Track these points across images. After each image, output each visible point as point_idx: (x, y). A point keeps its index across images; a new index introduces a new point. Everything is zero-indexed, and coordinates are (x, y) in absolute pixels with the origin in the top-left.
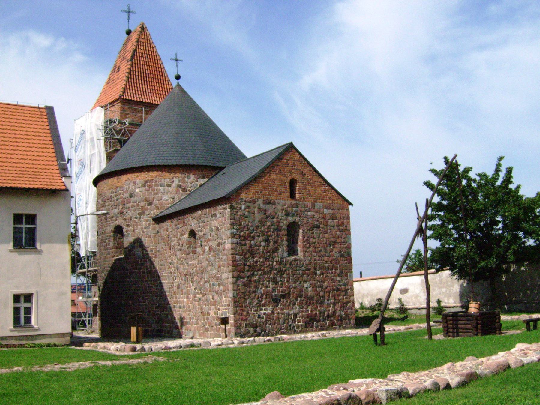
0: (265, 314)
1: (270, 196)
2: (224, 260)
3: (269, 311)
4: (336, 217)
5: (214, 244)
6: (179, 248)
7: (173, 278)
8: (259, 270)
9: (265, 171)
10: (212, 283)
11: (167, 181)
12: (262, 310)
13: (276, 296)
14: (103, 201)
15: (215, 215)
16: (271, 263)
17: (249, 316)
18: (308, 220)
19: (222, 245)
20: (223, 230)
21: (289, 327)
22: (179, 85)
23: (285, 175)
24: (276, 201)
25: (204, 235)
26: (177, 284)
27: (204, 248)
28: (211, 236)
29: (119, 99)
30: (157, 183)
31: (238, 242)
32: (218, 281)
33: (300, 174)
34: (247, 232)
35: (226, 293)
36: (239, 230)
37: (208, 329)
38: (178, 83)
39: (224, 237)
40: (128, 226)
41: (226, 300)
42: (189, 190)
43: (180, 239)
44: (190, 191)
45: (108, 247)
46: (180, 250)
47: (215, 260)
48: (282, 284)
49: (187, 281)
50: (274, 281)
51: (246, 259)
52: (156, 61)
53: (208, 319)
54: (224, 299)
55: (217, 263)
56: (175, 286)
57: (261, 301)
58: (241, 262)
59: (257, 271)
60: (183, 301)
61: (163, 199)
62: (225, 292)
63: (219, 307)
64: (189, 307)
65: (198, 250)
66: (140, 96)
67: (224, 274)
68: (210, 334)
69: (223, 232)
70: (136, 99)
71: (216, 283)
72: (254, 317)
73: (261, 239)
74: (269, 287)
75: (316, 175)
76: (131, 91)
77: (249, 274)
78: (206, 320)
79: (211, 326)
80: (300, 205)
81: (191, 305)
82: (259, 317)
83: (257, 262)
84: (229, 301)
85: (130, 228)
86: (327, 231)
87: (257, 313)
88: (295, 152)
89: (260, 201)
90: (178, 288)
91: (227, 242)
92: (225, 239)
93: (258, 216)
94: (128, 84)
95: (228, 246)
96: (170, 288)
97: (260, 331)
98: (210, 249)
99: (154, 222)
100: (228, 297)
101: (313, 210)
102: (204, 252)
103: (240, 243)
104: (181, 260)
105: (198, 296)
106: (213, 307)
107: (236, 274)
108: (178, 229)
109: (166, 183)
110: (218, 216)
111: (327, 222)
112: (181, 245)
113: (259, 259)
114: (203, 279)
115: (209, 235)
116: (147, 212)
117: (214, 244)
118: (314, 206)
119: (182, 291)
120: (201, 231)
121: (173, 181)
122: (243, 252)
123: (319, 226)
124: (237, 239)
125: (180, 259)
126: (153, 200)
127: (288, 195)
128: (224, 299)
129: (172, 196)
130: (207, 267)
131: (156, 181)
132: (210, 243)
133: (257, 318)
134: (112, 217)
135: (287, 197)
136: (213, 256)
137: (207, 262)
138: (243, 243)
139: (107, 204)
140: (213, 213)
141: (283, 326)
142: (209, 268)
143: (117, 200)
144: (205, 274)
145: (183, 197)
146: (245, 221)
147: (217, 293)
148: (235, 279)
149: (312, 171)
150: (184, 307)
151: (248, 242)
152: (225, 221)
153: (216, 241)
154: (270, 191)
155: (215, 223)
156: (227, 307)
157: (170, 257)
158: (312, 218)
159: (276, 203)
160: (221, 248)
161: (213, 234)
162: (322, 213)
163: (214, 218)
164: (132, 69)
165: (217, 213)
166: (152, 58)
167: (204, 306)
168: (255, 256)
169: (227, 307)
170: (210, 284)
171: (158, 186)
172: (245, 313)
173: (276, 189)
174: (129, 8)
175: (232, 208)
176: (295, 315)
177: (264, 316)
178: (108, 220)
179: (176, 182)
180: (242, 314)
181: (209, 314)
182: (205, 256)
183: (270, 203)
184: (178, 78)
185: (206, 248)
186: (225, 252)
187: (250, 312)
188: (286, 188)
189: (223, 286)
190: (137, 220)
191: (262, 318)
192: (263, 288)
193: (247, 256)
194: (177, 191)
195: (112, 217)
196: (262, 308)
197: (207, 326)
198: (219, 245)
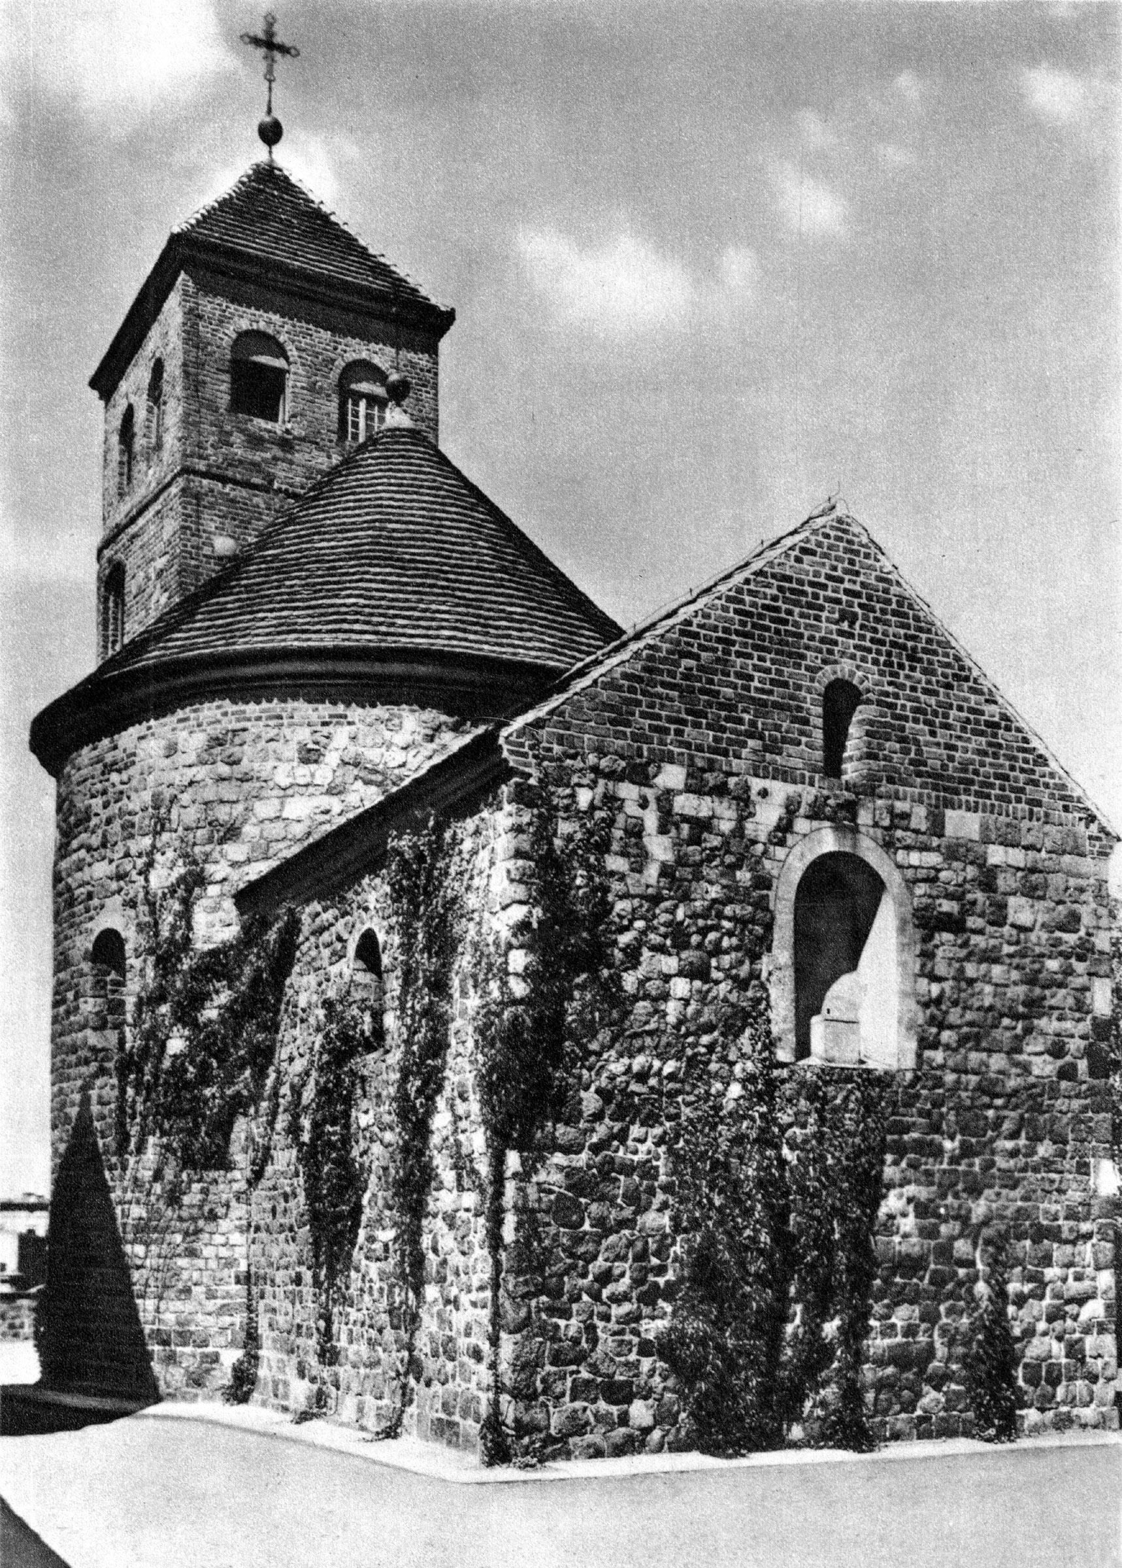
4: (1046, 886)
16: (718, 1086)
17: (594, 1341)
77: (601, 1130)
83: (642, 1077)
97: (648, 1421)
111: (1003, 906)
113: (657, 1064)
116: (217, 870)
118: (937, 826)
143: (109, 821)
154: (723, 729)
162: (980, 862)
168: (637, 1043)
173: (753, 724)
188: (806, 722)
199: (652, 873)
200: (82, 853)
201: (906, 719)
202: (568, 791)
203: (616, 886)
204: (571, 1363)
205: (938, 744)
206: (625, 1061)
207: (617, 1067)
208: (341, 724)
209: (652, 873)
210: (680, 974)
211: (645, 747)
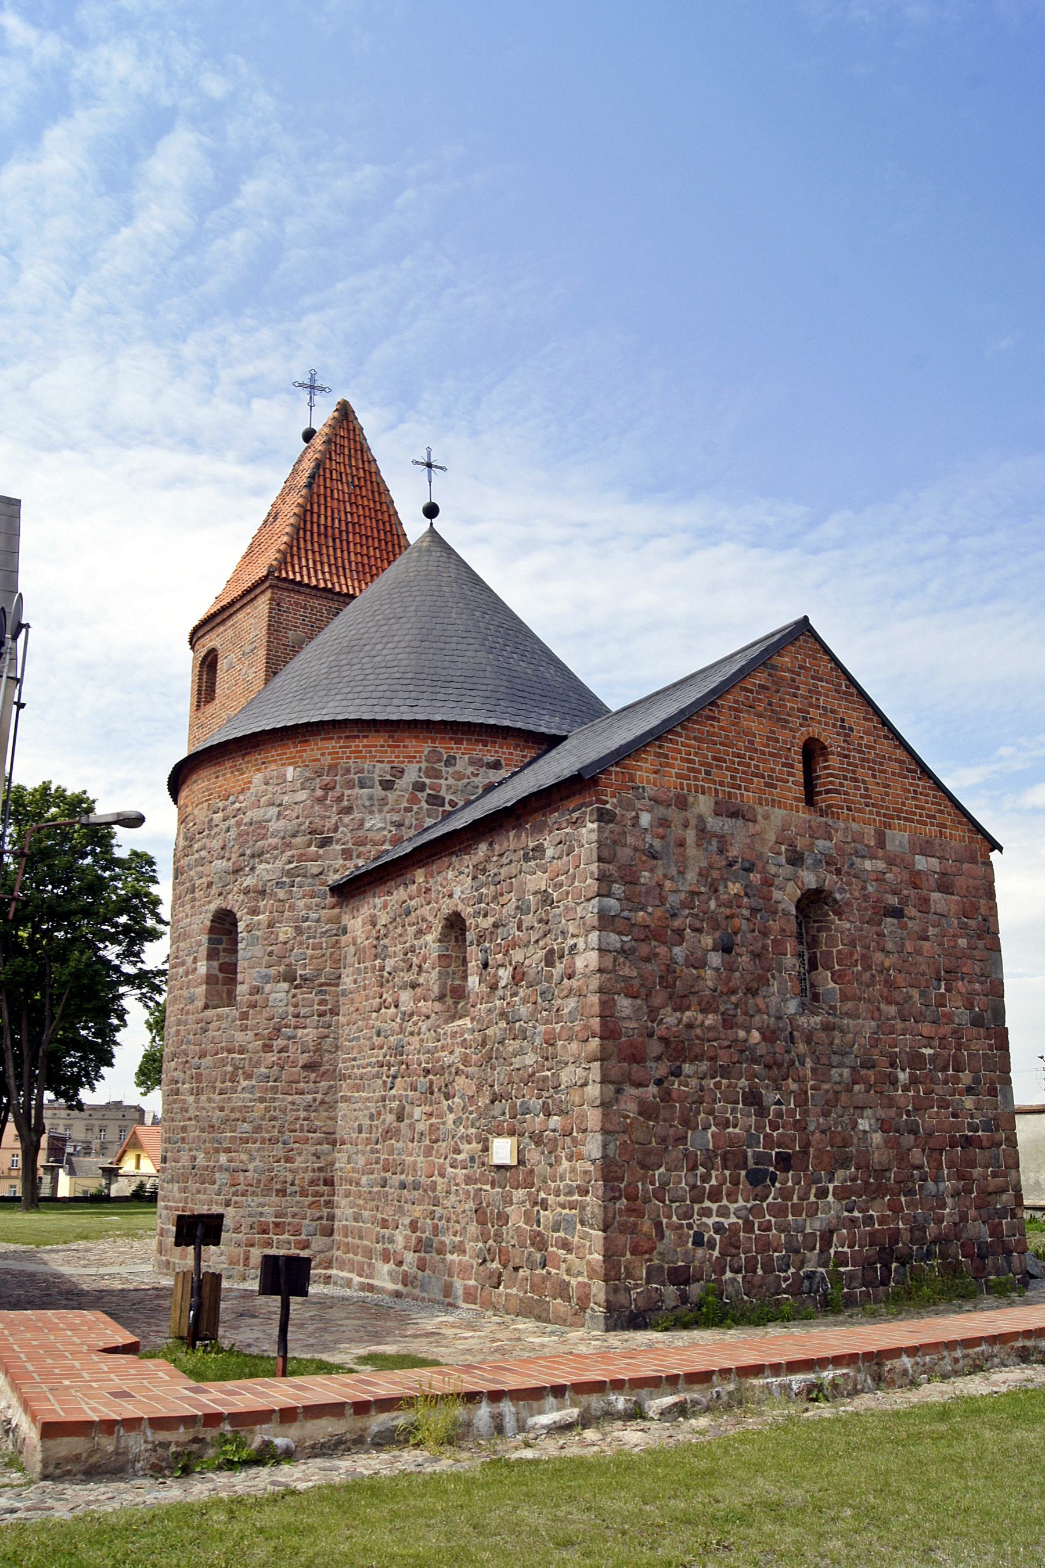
0: (718, 1228)
1: (739, 788)
2: (570, 1012)
3: (733, 1219)
5: (532, 958)
6: (409, 977)
7: (385, 1082)
8: (696, 1058)
9: (720, 702)
10: (519, 1102)
11: (381, 770)
12: (707, 1213)
13: (759, 1158)
14: (186, 839)
15: (539, 849)
16: (742, 1034)
17: (661, 1235)
18: (864, 888)
19: (562, 957)
20: (570, 901)
21: (806, 1283)
22: (432, 531)
23: (787, 721)
24: (760, 810)
25: (495, 926)
26: (395, 1104)
27: (495, 975)
28: (519, 929)
29: (266, 577)
30: (352, 776)
31: (627, 947)
32: (545, 1094)
33: (834, 726)
34: (659, 912)
35: (575, 1141)
36: (632, 902)
37: (500, 1275)
38: (431, 524)
39: (572, 929)
40: (254, 912)
41: (573, 1170)
42: (451, 801)
43: (412, 949)
44: (453, 804)
45: (190, 977)
46: (414, 986)
47: (533, 1017)
48: (779, 1114)
49: (432, 1093)
50: (753, 1099)
51: (653, 1013)
52: (376, 494)
53: (498, 1236)
54: (565, 1164)
55: (541, 1028)
56: (391, 1111)
57: (705, 1179)
58: (633, 1025)
59: (692, 1062)
60: (415, 1163)
61: (367, 825)
62: (568, 1139)
63: (542, 1195)
64: (433, 1187)
65: (473, 981)
66: (327, 576)
67: (571, 1068)
68: (507, 1294)
69: (566, 907)
70: (314, 582)
71: (536, 1103)
72: (681, 1241)
73: (708, 941)
74: (735, 1126)
75: (886, 737)
76: (304, 563)
77: (661, 1070)
78: (491, 1242)
79: (510, 1266)
80: (836, 831)
81: (439, 1180)
82: (698, 1241)
83: (690, 1026)
84: (585, 1172)
85: (261, 917)
86: (925, 930)
87: (690, 1226)
88: (817, 651)
89: (704, 805)
90: (400, 1118)
91: (581, 946)
92: (573, 936)
93: (696, 857)
94: (295, 542)
95: (587, 960)
96: (371, 1117)
98: (518, 976)
99: (334, 900)
100: (580, 1157)
101: (880, 853)
102: (494, 987)
103: (633, 950)
104: (415, 1018)
105: (465, 1147)
106: (519, 1194)
107: (617, 1068)
108: (408, 913)
109: (377, 778)
110: (549, 853)
112: (415, 968)
113: (700, 1017)
114: (486, 1088)
115: (513, 925)
117: (532, 958)
118: (881, 843)
119: (412, 1127)
120: (485, 915)
121: (402, 772)
122: (642, 985)
123: (902, 910)
124: (620, 933)
125: (412, 1015)
126: (336, 830)
127: (799, 791)
128: (565, 1164)
129: (396, 817)
130: (501, 1042)
131: (348, 771)
132: (517, 955)
133: (690, 1244)
134: (210, 885)
135: (797, 799)
136: (524, 1001)
137: (503, 1024)
138: (644, 949)
139: (196, 846)
140: (531, 845)
141: (786, 1279)
142: (512, 1045)
143: (228, 830)
144: (493, 1068)
145: (429, 822)
146: (652, 871)
147: (537, 1139)
148: (612, 1087)
149: (871, 720)
150: (416, 1186)
151: (662, 950)
152: (578, 866)
153: (541, 943)
154: (736, 770)
155: (537, 881)
156: (576, 1197)
157: (378, 1011)
158: (876, 880)
159: (759, 818)
160: (559, 968)
161: (529, 920)
163: (533, 863)
164: (309, 508)
165: (546, 844)
166: (365, 486)
167: (488, 1187)
168: (686, 1002)
169: (576, 1197)
170: (513, 1107)
171: (353, 788)
172: (646, 1226)
173: (757, 767)
174: (312, 379)
175: (604, 817)
176: (827, 1237)
177: (717, 1237)
178: (197, 895)
179: (412, 775)
180: (635, 1224)
181: (503, 1218)
182: (498, 1002)
183: (734, 814)
184: (431, 511)
185: (501, 972)
186: (574, 983)
187: (665, 1221)
188: (792, 766)
189: (562, 1113)
190: (281, 894)
191: (712, 1246)
192: (713, 1128)
193: (657, 1000)
194: (414, 800)
195: (210, 885)
196: (707, 1204)
197: (495, 1265)
198: (549, 960)
199: (691, 876)
200: (203, 853)
201: (856, 766)
202: (633, 814)
203: (668, 884)
204: (646, 1252)
205: (878, 784)
206: (678, 1014)
207: (671, 1020)
208: (412, 762)
209: (691, 876)
210: (714, 950)
211: (685, 782)
